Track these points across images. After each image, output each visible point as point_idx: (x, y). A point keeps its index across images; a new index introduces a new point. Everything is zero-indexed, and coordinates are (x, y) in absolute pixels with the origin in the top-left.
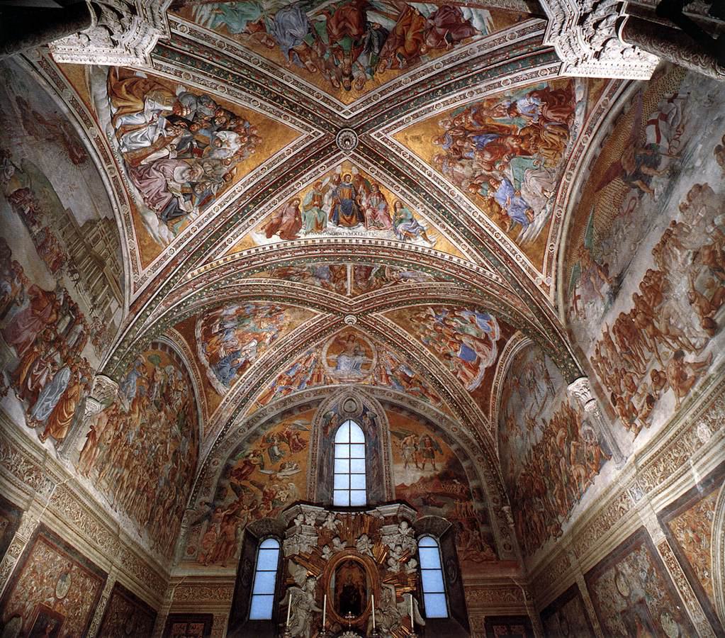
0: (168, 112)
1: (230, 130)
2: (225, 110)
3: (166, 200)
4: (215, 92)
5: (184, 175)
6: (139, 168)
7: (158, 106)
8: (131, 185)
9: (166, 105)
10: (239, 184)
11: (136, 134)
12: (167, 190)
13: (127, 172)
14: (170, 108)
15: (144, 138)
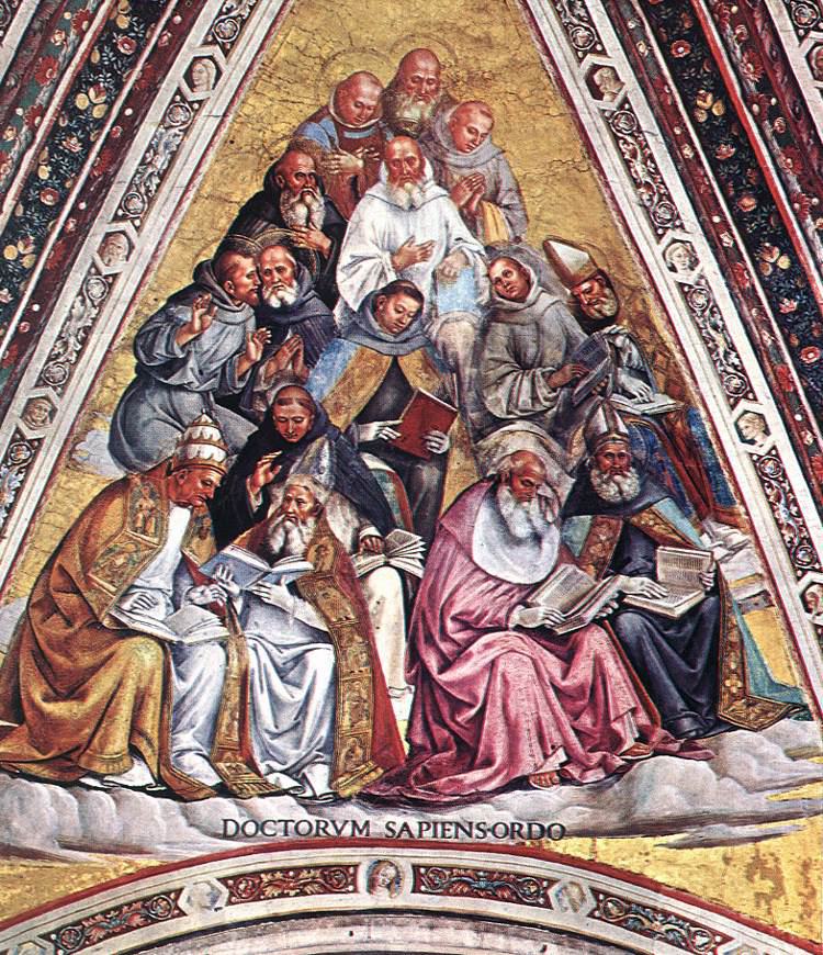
0: (193, 530)
1: (336, 229)
2: (227, 247)
3: (614, 669)
4: (124, 289)
5: (522, 530)
6: (418, 740)
7: (159, 574)
8: (476, 813)
9: (162, 532)
10: (652, 251)
11: (263, 702)
12: (559, 641)
13: (419, 805)
14: (179, 519)
15: (293, 669)
